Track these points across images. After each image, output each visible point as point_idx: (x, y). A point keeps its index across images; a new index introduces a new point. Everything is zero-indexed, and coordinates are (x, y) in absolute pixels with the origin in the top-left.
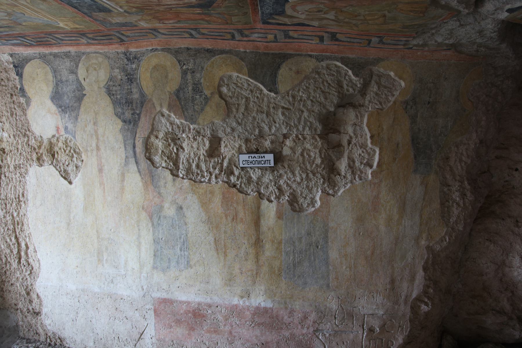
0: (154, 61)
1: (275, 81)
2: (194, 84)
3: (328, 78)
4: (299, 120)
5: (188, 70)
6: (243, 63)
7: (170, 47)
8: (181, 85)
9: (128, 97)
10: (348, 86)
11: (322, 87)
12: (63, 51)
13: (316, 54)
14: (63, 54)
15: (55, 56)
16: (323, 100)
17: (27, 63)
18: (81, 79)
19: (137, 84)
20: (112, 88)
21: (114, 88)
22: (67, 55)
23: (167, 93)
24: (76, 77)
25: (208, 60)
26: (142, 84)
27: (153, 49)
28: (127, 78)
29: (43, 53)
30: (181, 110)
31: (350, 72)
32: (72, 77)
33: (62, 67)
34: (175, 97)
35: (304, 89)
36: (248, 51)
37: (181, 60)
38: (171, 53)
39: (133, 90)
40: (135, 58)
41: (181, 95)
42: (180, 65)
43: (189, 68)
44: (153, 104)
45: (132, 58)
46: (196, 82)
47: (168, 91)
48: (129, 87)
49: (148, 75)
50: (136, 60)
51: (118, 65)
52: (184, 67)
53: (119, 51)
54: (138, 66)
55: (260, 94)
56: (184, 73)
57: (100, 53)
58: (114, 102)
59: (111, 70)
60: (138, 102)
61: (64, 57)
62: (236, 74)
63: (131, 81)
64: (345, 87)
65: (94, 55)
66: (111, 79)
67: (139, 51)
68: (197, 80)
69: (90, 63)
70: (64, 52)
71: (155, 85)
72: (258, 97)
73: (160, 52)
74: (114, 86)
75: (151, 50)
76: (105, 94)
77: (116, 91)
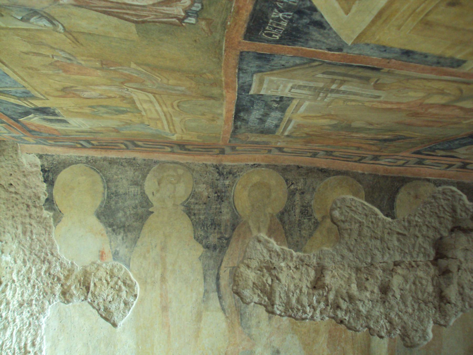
0: (256, 178)
1: (393, 206)
2: (303, 206)
3: (443, 202)
4: (414, 246)
5: (297, 190)
6: (360, 186)
8: (286, 206)
9: (216, 217)
10: (462, 211)
11: (438, 212)
12: (124, 157)
13: (434, 178)
14: (124, 160)
15: (112, 162)
16: (437, 225)
17: (64, 167)
18: (148, 192)
19: (229, 203)
20: (194, 207)
21: (197, 207)
22: (131, 162)
23: (268, 215)
24: (141, 189)
25: (322, 180)
26: (236, 203)
27: (254, 164)
29: (92, 157)
30: (284, 235)
31: (465, 197)
32: (134, 190)
33: (120, 176)
34: (278, 220)
35: (420, 214)
36: (366, 173)
37: (289, 179)
38: (278, 170)
39: (222, 210)
40: (230, 173)
41: (286, 218)
42: (287, 184)
43: (298, 188)
44: (249, 227)
45: (225, 173)
46: (305, 204)
47: (270, 213)
48: (219, 206)
49: (246, 193)
50: (231, 176)
51: (206, 179)
52: (292, 187)
53: (209, 163)
54: (233, 183)
55: (375, 218)
56: (292, 194)
57: (181, 164)
58: (195, 224)
59: (195, 185)
60: (229, 224)
61: (126, 164)
62: (351, 197)
63: (222, 199)
64: (459, 211)
65: (172, 165)
66: (193, 195)
67: (236, 165)
68: (306, 202)
69: (165, 174)
70: (125, 159)
71: (253, 206)
72: (372, 222)
73: (263, 169)
74: (196, 203)
75: (252, 165)
76: (183, 212)
77: (199, 210)
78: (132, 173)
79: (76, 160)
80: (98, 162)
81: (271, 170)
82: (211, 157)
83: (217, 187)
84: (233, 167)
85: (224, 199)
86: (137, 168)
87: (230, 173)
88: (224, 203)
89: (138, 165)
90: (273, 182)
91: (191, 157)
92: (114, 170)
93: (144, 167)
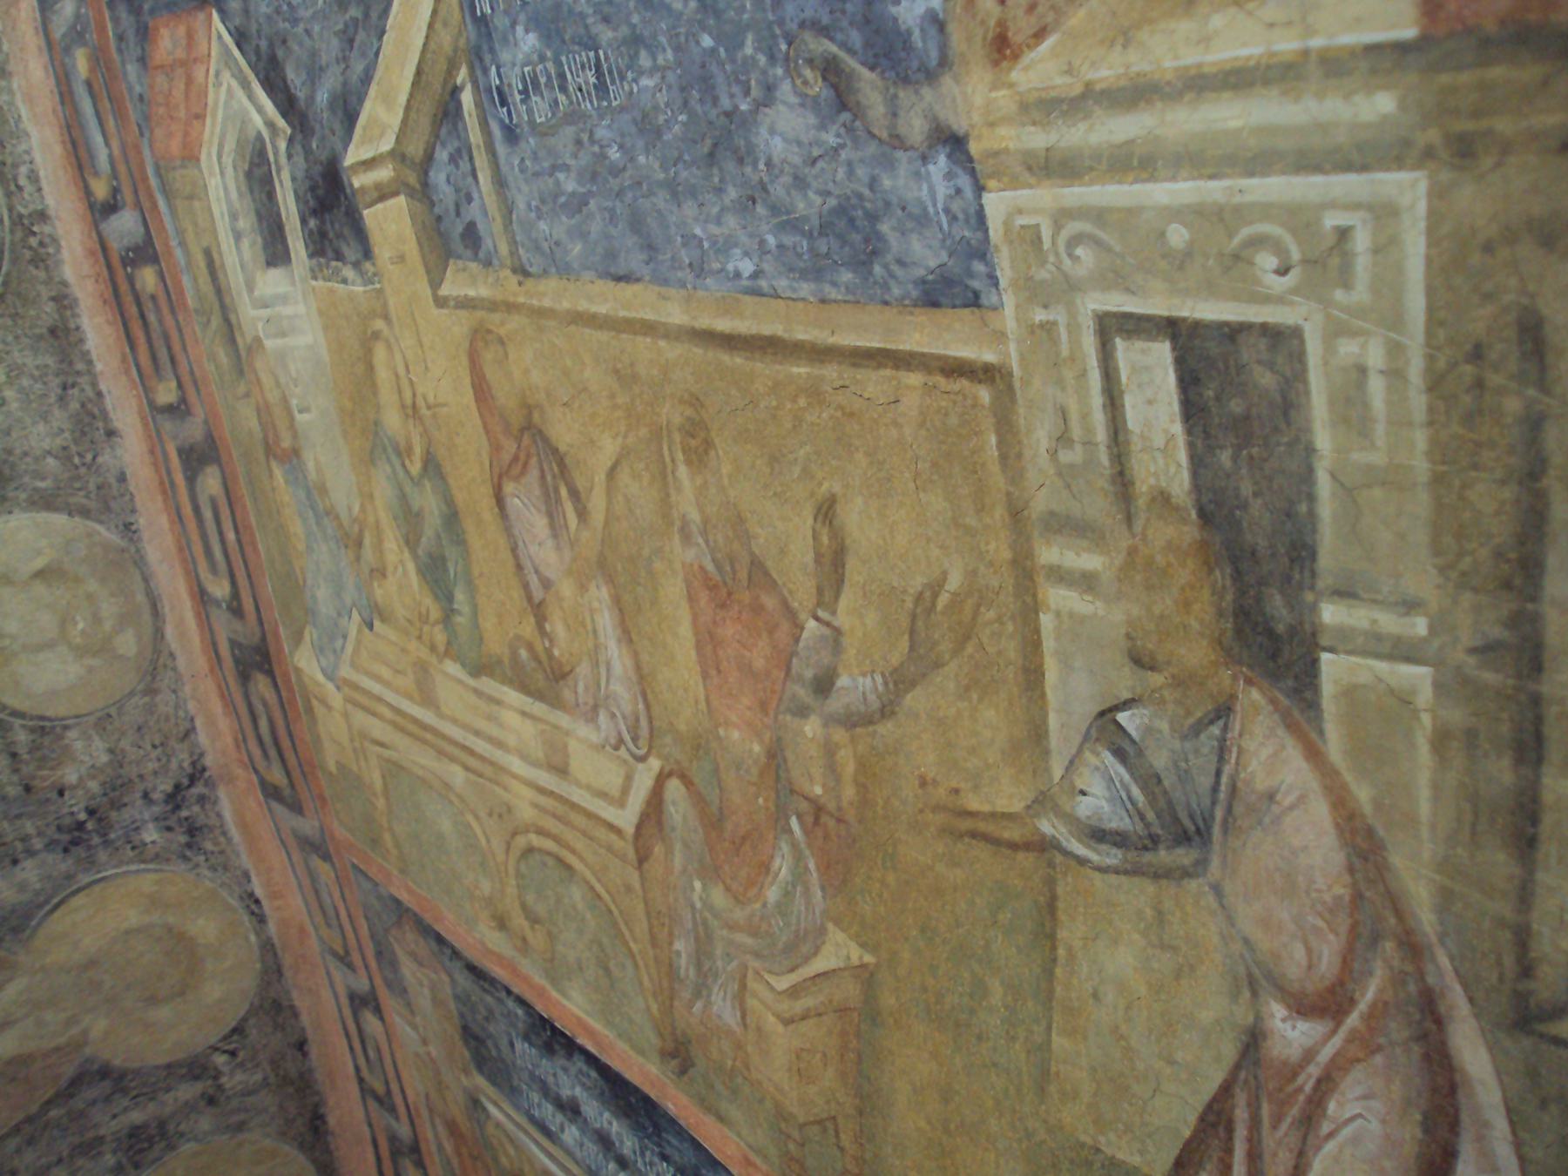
0: (204, 928)
2: (162, 1125)
5: (216, 1078)
7: (288, 974)
8: (137, 1072)
12: (103, 387)
14: (90, 392)
15: (62, 336)
19: (70, 877)
23: (74, 1031)
25: (282, 1134)
27: (257, 902)
28: (82, 816)
29: (55, 240)
30: (20, 1116)
34: (69, 1071)
37: (246, 1037)
39: (28, 864)
40: (193, 831)
41: (90, 1093)
42: (225, 1038)
43: (224, 1080)
45: (184, 813)
46: (171, 1127)
47: (85, 1033)
48: (38, 844)
49: (133, 918)
50: (183, 839)
51: (133, 754)
52: (220, 1059)
53: (203, 738)
54: (157, 856)
56: (196, 1068)
57: (159, 634)
59: (92, 719)
61: (74, 405)
63: (75, 842)
65: (140, 598)
66: (46, 730)
67: (229, 840)
68: (182, 1127)
69: (92, 586)
70: (99, 394)
71: (92, 963)
73: (253, 938)
74: (14, 755)
75: (251, 895)
78: (46, 445)
79: (15, 166)
80: (42, 275)
81: (258, 966)
82: (229, 740)
83: (118, 805)
84: (217, 832)
85: (80, 851)
86: (76, 460)
87: (193, 831)
88: (61, 856)
89: (89, 457)
90: (213, 991)
91: (202, 663)
92: (30, 361)
93: (92, 486)
